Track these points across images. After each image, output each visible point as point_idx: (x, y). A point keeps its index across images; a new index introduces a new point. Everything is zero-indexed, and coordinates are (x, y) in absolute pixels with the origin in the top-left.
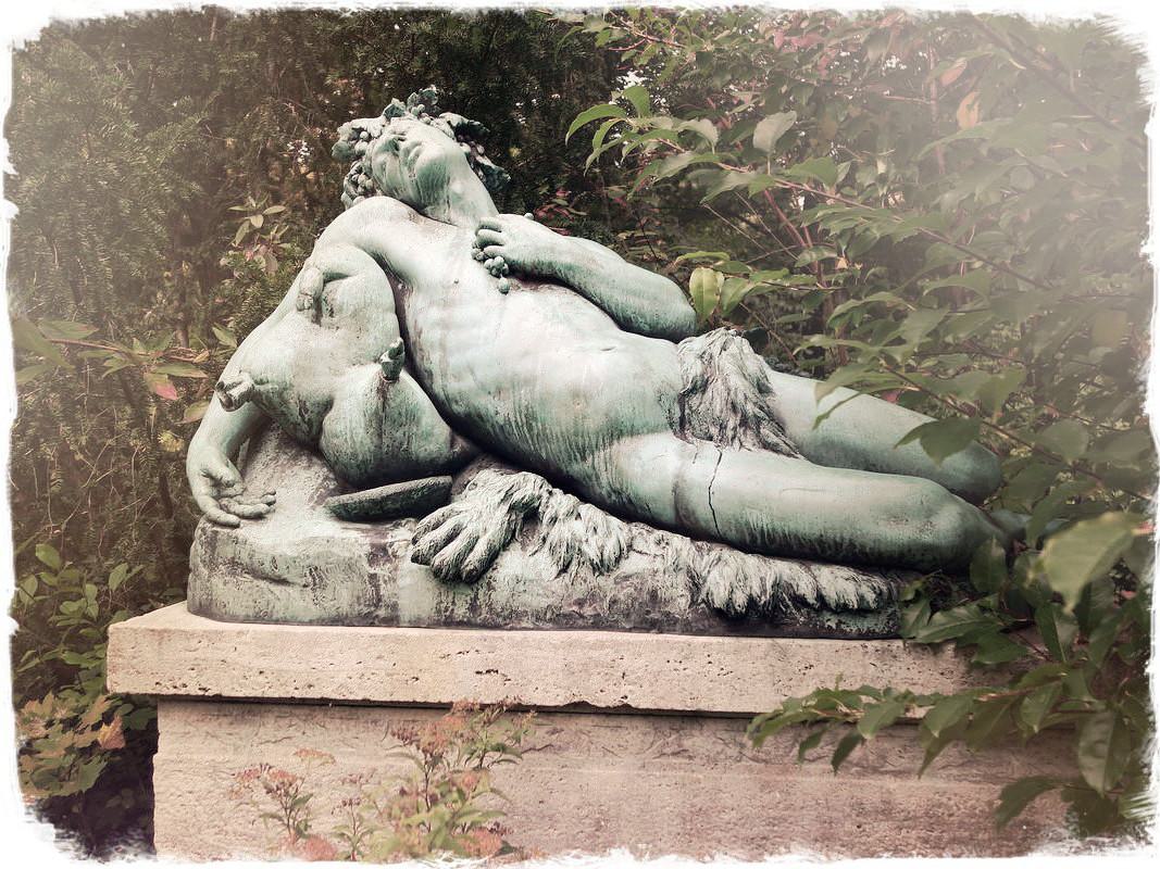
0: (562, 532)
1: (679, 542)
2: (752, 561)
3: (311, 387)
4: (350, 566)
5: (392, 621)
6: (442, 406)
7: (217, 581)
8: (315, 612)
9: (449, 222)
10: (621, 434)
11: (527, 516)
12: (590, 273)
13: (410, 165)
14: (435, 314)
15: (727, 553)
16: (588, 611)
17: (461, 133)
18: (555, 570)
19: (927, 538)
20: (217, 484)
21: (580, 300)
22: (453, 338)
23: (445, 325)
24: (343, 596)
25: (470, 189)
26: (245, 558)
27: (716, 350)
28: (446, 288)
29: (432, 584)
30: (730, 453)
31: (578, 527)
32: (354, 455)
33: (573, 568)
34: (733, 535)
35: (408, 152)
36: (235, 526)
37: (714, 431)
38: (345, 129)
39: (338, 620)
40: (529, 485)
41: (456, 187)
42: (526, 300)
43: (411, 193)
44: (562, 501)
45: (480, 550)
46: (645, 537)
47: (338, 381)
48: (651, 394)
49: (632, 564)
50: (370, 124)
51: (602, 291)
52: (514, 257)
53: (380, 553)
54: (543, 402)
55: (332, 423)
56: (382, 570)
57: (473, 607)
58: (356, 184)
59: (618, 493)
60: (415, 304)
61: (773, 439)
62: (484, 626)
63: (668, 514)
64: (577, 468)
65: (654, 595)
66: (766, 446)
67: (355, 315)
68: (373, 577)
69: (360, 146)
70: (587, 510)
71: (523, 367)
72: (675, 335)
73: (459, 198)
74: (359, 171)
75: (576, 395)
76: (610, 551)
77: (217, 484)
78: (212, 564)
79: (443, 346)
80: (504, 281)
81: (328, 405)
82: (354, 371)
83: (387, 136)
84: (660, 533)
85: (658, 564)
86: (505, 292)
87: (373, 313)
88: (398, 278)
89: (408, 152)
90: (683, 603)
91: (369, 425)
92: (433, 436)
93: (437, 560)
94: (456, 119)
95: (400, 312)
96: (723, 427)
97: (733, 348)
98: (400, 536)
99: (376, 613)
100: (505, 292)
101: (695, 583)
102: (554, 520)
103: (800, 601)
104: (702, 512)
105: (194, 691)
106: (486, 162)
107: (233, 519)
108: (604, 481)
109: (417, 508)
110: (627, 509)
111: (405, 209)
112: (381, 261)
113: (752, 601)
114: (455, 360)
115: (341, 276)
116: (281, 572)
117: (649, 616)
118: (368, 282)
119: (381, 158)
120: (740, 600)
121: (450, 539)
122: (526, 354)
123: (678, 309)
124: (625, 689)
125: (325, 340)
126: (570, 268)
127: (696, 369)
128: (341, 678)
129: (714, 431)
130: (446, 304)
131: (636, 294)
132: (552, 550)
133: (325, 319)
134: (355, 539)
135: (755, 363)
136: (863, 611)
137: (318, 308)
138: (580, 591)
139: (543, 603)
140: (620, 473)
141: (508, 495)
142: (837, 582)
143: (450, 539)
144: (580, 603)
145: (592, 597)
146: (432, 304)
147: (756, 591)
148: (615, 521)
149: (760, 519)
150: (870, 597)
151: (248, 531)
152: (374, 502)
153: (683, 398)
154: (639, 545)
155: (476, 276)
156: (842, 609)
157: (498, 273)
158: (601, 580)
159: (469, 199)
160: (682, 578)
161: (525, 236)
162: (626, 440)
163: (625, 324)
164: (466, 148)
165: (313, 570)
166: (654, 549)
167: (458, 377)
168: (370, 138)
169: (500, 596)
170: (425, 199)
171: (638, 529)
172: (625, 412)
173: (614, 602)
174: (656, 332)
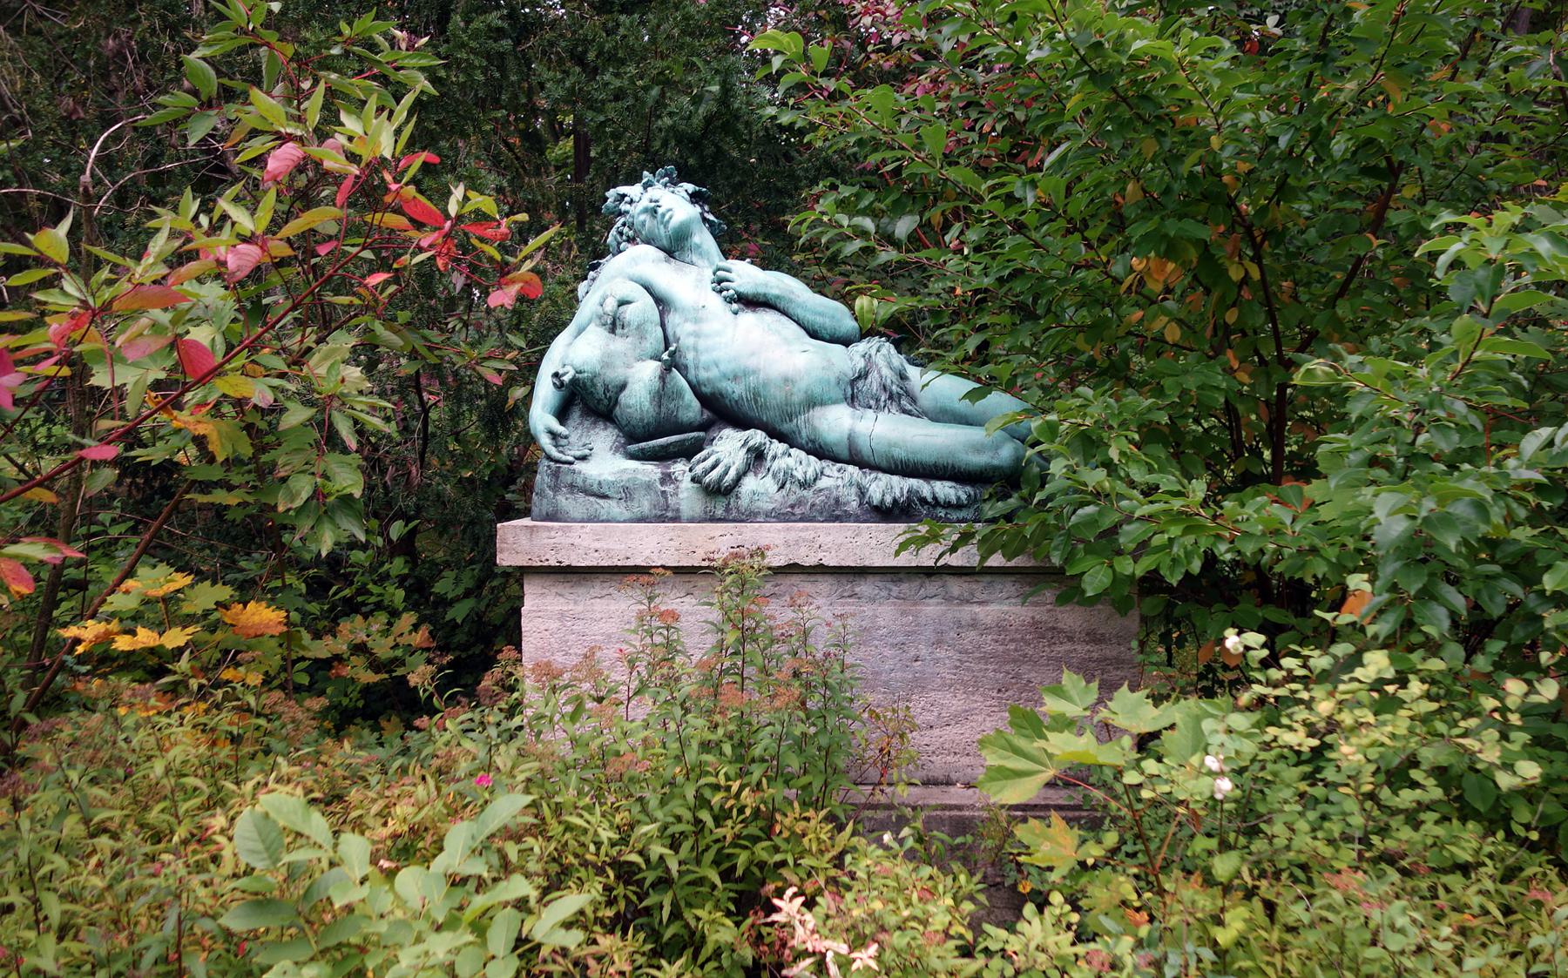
0: (781, 463)
1: (851, 468)
2: (895, 479)
3: (614, 375)
4: (649, 486)
5: (676, 519)
6: (696, 389)
7: (561, 498)
8: (627, 515)
9: (692, 263)
10: (814, 405)
11: (757, 457)
12: (791, 301)
13: (666, 225)
14: (689, 327)
15: (880, 475)
16: (797, 511)
17: (695, 198)
18: (776, 488)
19: (996, 462)
20: (554, 436)
21: (784, 319)
22: (702, 344)
23: (697, 335)
24: (645, 505)
25: (704, 239)
26: (579, 482)
27: (873, 352)
28: (696, 310)
29: (701, 496)
30: (882, 416)
31: (790, 462)
32: (642, 420)
33: (788, 485)
34: (884, 464)
35: (663, 215)
36: (571, 463)
37: (872, 403)
38: (612, 194)
39: (642, 519)
40: (757, 437)
41: (696, 239)
42: (749, 318)
43: (665, 243)
44: (777, 447)
45: (732, 474)
46: (831, 469)
47: (630, 372)
48: (833, 380)
49: (823, 483)
50: (634, 191)
51: (800, 312)
52: (741, 290)
53: (667, 478)
54: (765, 385)
55: (624, 398)
56: (669, 489)
57: (727, 510)
58: (621, 234)
59: (813, 442)
60: (673, 320)
61: (909, 407)
62: (734, 521)
63: (845, 454)
64: (786, 427)
65: (837, 501)
66: (905, 411)
67: (638, 327)
68: (664, 492)
69: (624, 207)
70: (794, 451)
71: (752, 363)
72: (846, 342)
73: (699, 246)
74: (624, 225)
75: (786, 380)
76: (810, 474)
77: (554, 436)
78: (556, 488)
79: (695, 349)
80: (735, 306)
81: (623, 387)
82: (639, 365)
83: (645, 203)
84: (839, 465)
85: (840, 482)
86: (736, 313)
87: (649, 327)
88: (662, 302)
89: (663, 215)
90: (855, 504)
91: (652, 399)
92: (691, 408)
93: (707, 479)
94: (691, 187)
95: (663, 325)
96: (878, 400)
97: (884, 351)
98: (679, 468)
99: (666, 515)
100: (736, 313)
101: (862, 492)
102: (774, 458)
103: (923, 501)
104: (866, 451)
105: (553, 563)
106: (711, 217)
107: (570, 459)
108: (804, 434)
109: (687, 452)
110: (820, 451)
111: (662, 254)
112: (648, 289)
113: (895, 501)
114: (704, 358)
115: (628, 303)
116: (605, 490)
117: (834, 513)
118: (643, 306)
119: (642, 217)
120: (888, 499)
121: (714, 467)
122: (753, 354)
123: (848, 324)
124: (820, 555)
125: (619, 344)
126: (778, 297)
127: (861, 364)
128: (647, 553)
129: (872, 403)
130: (697, 321)
131: (821, 314)
132: (774, 476)
133: (619, 331)
134: (651, 471)
135: (898, 360)
136: (959, 506)
137: (614, 325)
138: (792, 499)
139: (771, 506)
140: (814, 429)
141: (746, 442)
142: (945, 490)
143: (714, 467)
144: (792, 506)
145: (800, 502)
146: (686, 320)
147: (898, 494)
148: (812, 458)
149: (899, 453)
150: (964, 497)
151: (578, 466)
152: (662, 447)
153: (853, 382)
154: (827, 471)
155: (716, 302)
156: (948, 505)
157: (730, 300)
158: (805, 493)
159: (705, 247)
160: (854, 490)
161: (747, 275)
162: (818, 409)
163: (814, 334)
164: (698, 209)
165: (626, 489)
166: (836, 474)
167: (707, 369)
168: (631, 202)
169: (744, 502)
170: (675, 247)
171: (825, 463)
172: (817, 390)
173: (813, 505)
174: (833, 340)
